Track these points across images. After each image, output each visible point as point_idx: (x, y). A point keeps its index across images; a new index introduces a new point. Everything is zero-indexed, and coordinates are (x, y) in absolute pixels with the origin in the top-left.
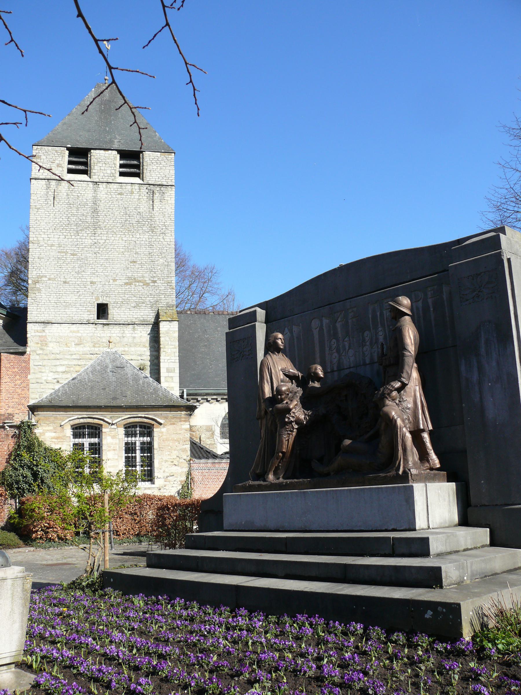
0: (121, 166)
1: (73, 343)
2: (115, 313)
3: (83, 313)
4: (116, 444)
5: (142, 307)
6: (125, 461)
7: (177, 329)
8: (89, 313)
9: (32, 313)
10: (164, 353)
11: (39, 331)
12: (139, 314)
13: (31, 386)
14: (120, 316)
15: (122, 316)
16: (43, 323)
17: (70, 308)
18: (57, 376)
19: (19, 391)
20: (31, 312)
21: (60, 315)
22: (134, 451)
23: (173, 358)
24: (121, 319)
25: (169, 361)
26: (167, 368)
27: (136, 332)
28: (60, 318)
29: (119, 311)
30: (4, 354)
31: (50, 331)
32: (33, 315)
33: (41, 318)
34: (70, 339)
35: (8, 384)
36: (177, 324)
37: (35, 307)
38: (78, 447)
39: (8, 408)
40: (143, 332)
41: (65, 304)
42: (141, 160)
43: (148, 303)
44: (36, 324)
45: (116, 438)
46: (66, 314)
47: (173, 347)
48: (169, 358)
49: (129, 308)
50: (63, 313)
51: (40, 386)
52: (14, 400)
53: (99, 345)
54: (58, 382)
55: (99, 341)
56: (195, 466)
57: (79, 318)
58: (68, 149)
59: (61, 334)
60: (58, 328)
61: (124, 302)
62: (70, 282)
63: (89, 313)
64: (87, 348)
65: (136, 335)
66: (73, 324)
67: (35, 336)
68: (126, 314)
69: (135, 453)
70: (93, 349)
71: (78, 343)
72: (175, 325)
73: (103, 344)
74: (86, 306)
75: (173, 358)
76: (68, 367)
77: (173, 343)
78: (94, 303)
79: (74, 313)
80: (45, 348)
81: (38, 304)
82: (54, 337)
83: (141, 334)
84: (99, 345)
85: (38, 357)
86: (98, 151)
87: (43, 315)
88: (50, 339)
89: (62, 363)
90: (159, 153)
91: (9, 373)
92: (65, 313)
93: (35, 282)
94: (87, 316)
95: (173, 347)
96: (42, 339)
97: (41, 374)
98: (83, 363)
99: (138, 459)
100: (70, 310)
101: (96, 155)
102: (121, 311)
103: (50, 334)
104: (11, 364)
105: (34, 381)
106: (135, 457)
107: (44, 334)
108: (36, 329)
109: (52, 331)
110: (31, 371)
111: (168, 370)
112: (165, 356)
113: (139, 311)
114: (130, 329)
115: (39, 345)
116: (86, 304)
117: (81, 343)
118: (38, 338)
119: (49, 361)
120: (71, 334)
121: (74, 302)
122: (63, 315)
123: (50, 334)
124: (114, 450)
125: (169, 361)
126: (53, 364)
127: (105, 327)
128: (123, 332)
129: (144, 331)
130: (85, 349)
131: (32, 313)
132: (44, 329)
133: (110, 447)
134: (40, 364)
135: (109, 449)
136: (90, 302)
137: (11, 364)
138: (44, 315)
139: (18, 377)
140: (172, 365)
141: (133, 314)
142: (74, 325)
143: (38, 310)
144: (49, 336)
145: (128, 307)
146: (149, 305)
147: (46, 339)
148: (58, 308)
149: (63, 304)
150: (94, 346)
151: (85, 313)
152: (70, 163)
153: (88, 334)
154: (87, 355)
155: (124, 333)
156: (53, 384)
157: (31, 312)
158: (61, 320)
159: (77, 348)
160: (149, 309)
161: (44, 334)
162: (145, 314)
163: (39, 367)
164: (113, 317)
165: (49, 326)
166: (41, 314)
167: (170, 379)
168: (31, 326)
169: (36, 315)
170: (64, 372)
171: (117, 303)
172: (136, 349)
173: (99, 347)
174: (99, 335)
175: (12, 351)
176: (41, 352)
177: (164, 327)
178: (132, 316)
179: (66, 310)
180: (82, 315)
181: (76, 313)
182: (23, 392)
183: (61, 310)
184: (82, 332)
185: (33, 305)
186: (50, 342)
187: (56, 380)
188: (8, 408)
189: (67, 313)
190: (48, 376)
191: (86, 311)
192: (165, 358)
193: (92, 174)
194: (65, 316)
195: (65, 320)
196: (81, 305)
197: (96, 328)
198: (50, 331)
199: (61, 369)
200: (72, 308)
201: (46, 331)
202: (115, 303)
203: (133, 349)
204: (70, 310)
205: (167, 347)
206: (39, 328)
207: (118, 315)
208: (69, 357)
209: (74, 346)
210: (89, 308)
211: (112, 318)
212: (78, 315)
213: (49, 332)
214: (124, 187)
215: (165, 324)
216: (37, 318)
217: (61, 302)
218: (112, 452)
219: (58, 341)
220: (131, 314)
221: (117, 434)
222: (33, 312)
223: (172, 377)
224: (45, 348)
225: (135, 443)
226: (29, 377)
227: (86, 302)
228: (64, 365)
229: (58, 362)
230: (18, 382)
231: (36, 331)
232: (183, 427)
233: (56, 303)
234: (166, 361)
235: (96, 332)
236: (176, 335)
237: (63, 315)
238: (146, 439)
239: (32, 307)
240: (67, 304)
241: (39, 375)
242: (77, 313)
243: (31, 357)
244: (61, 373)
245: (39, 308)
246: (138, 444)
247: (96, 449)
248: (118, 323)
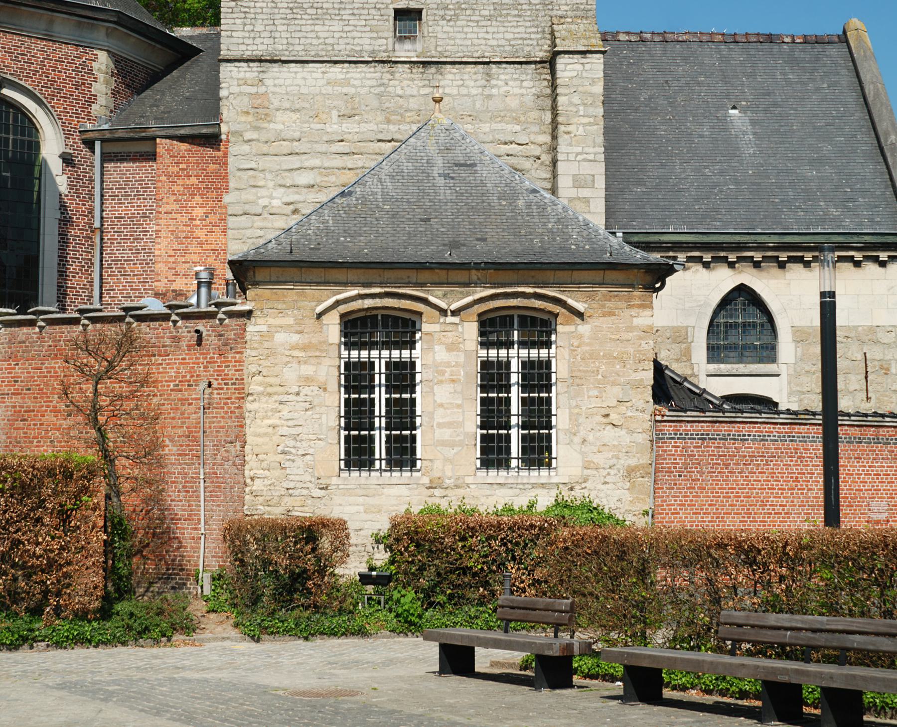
1: (335, 113)
2: (439, 36)
3: (359, 35)
4: (457, 365)
5: (510, 18)
6: (482, 410)
7: (601, 74)
8: (375, 35)
9: (232, 37)
10: (566, 136)
11: (249, 82)
12: (501, 36)
13: (232, 222)
14: (452, 42)
15: (458, 42)
16: (261, 61)
17: (327, 22)
18: (296, 198)
19: (201, 233)
20: (229, 33)
21: (302, 41)
23: (591, 150)
24: (455, 48)
25: (579, 158)
26: (574, 175)
27: (494, 82)
28: (302, 47)
29: (451, 30)
30: (164, 141)
31: (276, 82)
32: (233, 40)
33: (255, 47)
34: (328, 102)
35: (174, 215)
36: (602, 61)
37: (238, 21)
39: (173, 278)
40: (510, 83)
41: (313, 11)
43: (525, 7)
44: (242, 64)
45: (458, 350)
46: (318, 38)
47: (592, 120)
48: (579, 149)
49: (478, 22)
50: (309, 35)
51: (253, 222)
52: (188, 257)
53: (399, 118)
55: (401, 107)
57: (349, 47)
59: (304, 90)
60: (296, 72)
61: (463, 6)
63: (375, 35)
64: (370, 126)
65: (494, 91)
66: (336, 62)
67: (240, 94)
68: (469, 36)
70: (385, 126)
71: (347, 112)
72: (597, 63)
73: (409, 114)
74: (368, 18)
75: (591, 150)
76: (320, 174)
77: (591, 110)
78: (387, 8)
79: (337, 35)
80: (266, 125)
81: (245, 12)
82: (286, 97)
83: (506, 88)
84: (399, 118)
85: (246, 148)
87: (258, 41)
88: (276, 103)
89: (307, 164)
91: (174, 188)
92: (313, 35)
94: (368, 41)
95: (592, 120)
96: (259, 101)
97: (254, 190)
98: (360, 164)
100: (327, 28)
102: (456, 29)
103: (278, 90)
104: (181, 166)
105: (237, 209)
106: (508, 400)
107: (262, 89)
108: (242, 75)
109: (281, 82)
110: (232, 185)
111: (578, 182)
112: (570, 145)
113: (502, 29)
114: (479, 76)
115: (250, 118)
116: (366, 12)
117: (354, 112)
118: (246, 99)
119: (275, 158)
120: (329, 89)
121: (336, 6)
122: (309, 41)
123: (278, 90)
124: (453, 381)
125: (579, 158)
126: (285, 167)
127: (414, 71)
128: (461, 82)
129: (516, 79)
130: (364, 127)
131: (232, 37)
132: (262, 76)
133: (443, 373)
134: (253, 165)
135: (440, 378)
136: (378, 6)
137: (181, 166)
138: (261, 40)
139: (198, 199)
140: (587, 169)
141: (487, 36)
142: (337, 65)
143: (248, 28)
144: (274, 93)
145: (472, 18)
146: (529, 13)
147: (266, 103)
148: (296, 22)
149: (309, 11)
150: (388, 122)
151: (363, 35)
153: (372, 90)
154: (371, 144)
155: (463, 85)
156: (285, 218)
157: (229, 33)
158: (303, 53)
159: (344, 125)
160: (528, 24)
161: (262, 89)
162: (516, 35)
163: (251, 173)
164: (437, 46)
165: (276, 69)
166: (254, 38)
167: (583, 205)
168: (229, 69)
169: (241, 41)
170: (313, 186)
171: (446, 8)
172: (495, 126)
173: (400, 122)
174: (400, 92)
175: (182, 132)
176: (254, 135)
177: (566, 67)
178: (484, 42)
179: (317, 28)
180: (356, 41)
181: (341, 34)
182: (212, 238)
183: (303, 28)
184: (356, 83)
185: (235, 16)
186: (278, 110)
187: (291, 207)
188: (173, 278)
189: (321, 35)
190: (271, 197)
191: (368, 28)
192: (570, 149)
194: (315, 42)
195: (313, 53)
196: (353, 14)
197: (392, 73)
198: (276, 82)
199: (304, 179)
200: (331, 23)
201: (268, 82)
202: (441, 6)
203: (486, 127)
204: (327, 28)
205: (575, 120)
206: (248, 75)
207: (449, 38)
208: (323, 148)
209: (335, 118)
210: (374, 23)
211: (433, 48)
212: (347, 41)
213: (275, 85)
215: (571, 61)
216: (243, 47)
217: (305, 6)
218: (449, 387)
219: (297, 106)
220: (480, 35)
221: (461, 340)
222: (234, 34)
223: (587, 201)
224: (266, 125)
225: (508, 363)
226: (227, 199)
227: (366, 6)
228: (312, 169)
229: (295, 162)
230: (199, 212)
231: (241, 82)
232: (637, 321)
233: (291, 9)
234: (572, 157)
235: (392, 83)
236: (599, 88)
237: (309, 41)
239: (232, 21)
240: (320, 11)
241: (247, 196)
242: (344, 35)
243: (233, 150)
244: (306, 190)
245: (248, 21)
248: (448, 60)
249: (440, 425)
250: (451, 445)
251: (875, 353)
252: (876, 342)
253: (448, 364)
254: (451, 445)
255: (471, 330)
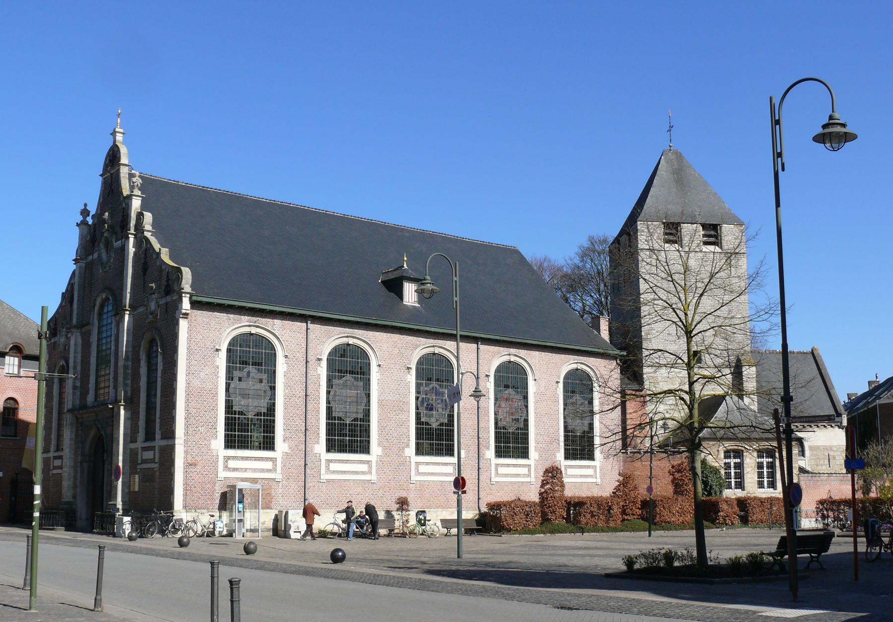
0: (704, 236)
22: (763, 468)
38: (727, 466)
42: (719, 232)
54: (667, 412)
56: (802, 478)
58: (664, 223)
62: (673, 334)
69: (763, 469)
86: (686, 225)
88: (660, 379)
90: (733, 226)
93: (647, 334)
99: (765, 473)
101: (687, 229)
106: (763, 472)
152: (666, 234)
175: (634, 388)
187: (666, 411)
193: (683, 244)
214: (708, 255)
238: (770, 460)
246: (765, 463)
247: (739, 466)
249: (750, 478)
250: (751, 483)
251: (831, 453)
252: (831, 450)
253: (750, 463)
254: (751, 483)
255: (755, 454)
